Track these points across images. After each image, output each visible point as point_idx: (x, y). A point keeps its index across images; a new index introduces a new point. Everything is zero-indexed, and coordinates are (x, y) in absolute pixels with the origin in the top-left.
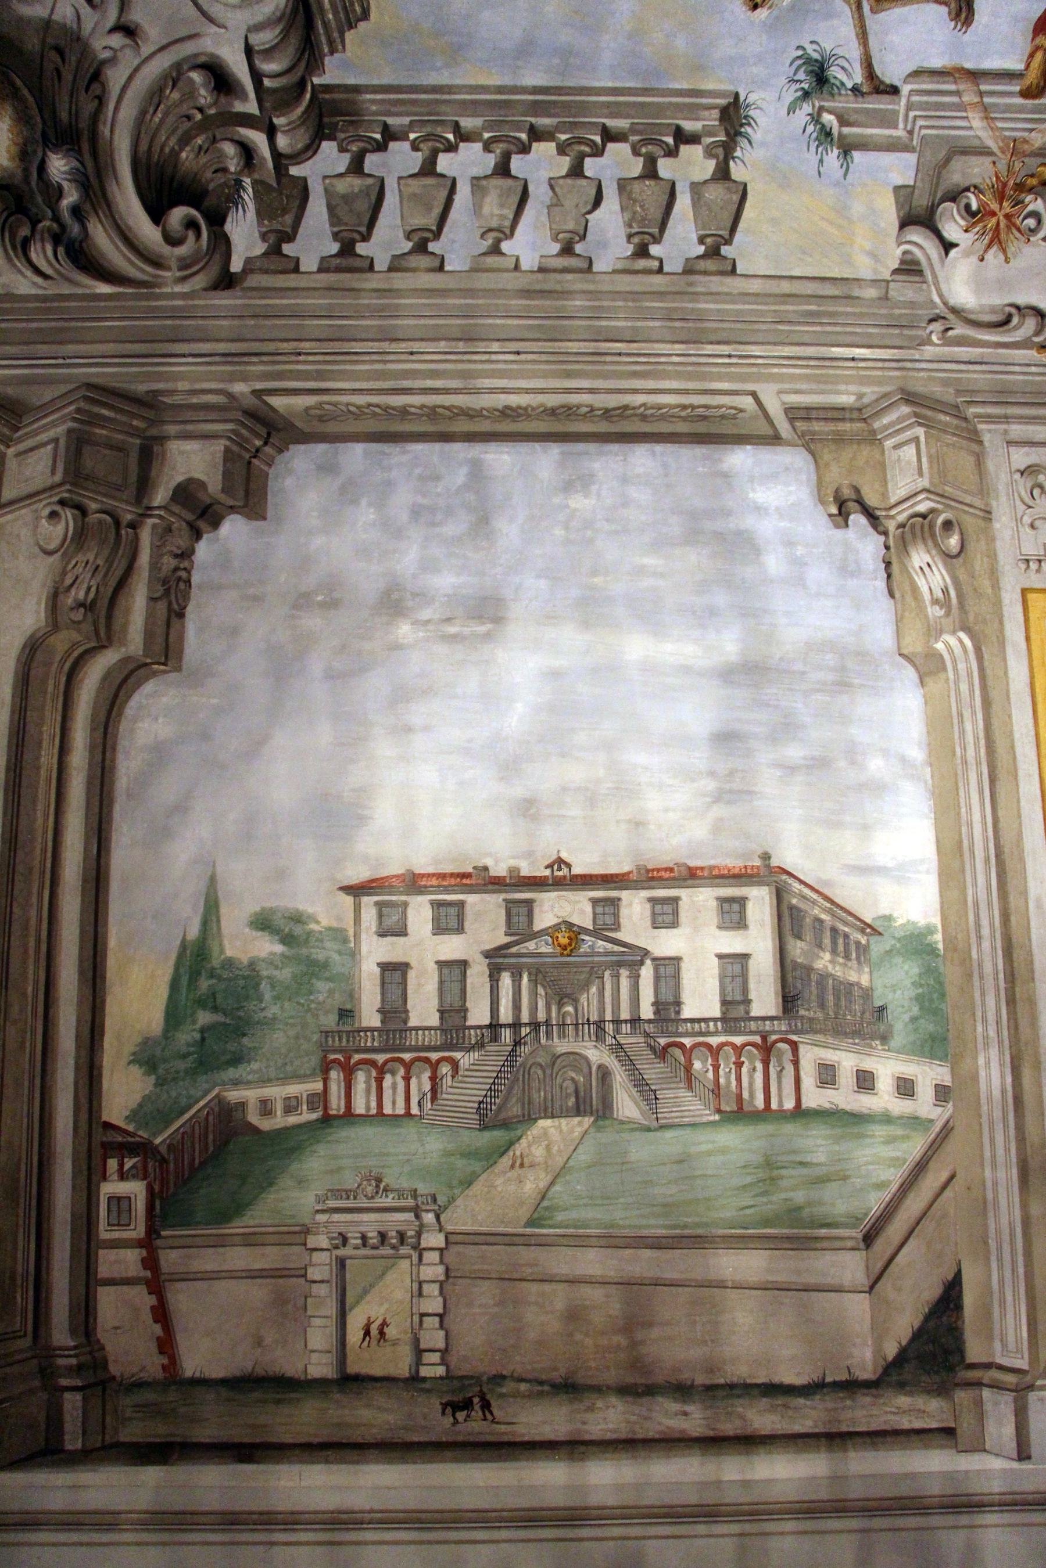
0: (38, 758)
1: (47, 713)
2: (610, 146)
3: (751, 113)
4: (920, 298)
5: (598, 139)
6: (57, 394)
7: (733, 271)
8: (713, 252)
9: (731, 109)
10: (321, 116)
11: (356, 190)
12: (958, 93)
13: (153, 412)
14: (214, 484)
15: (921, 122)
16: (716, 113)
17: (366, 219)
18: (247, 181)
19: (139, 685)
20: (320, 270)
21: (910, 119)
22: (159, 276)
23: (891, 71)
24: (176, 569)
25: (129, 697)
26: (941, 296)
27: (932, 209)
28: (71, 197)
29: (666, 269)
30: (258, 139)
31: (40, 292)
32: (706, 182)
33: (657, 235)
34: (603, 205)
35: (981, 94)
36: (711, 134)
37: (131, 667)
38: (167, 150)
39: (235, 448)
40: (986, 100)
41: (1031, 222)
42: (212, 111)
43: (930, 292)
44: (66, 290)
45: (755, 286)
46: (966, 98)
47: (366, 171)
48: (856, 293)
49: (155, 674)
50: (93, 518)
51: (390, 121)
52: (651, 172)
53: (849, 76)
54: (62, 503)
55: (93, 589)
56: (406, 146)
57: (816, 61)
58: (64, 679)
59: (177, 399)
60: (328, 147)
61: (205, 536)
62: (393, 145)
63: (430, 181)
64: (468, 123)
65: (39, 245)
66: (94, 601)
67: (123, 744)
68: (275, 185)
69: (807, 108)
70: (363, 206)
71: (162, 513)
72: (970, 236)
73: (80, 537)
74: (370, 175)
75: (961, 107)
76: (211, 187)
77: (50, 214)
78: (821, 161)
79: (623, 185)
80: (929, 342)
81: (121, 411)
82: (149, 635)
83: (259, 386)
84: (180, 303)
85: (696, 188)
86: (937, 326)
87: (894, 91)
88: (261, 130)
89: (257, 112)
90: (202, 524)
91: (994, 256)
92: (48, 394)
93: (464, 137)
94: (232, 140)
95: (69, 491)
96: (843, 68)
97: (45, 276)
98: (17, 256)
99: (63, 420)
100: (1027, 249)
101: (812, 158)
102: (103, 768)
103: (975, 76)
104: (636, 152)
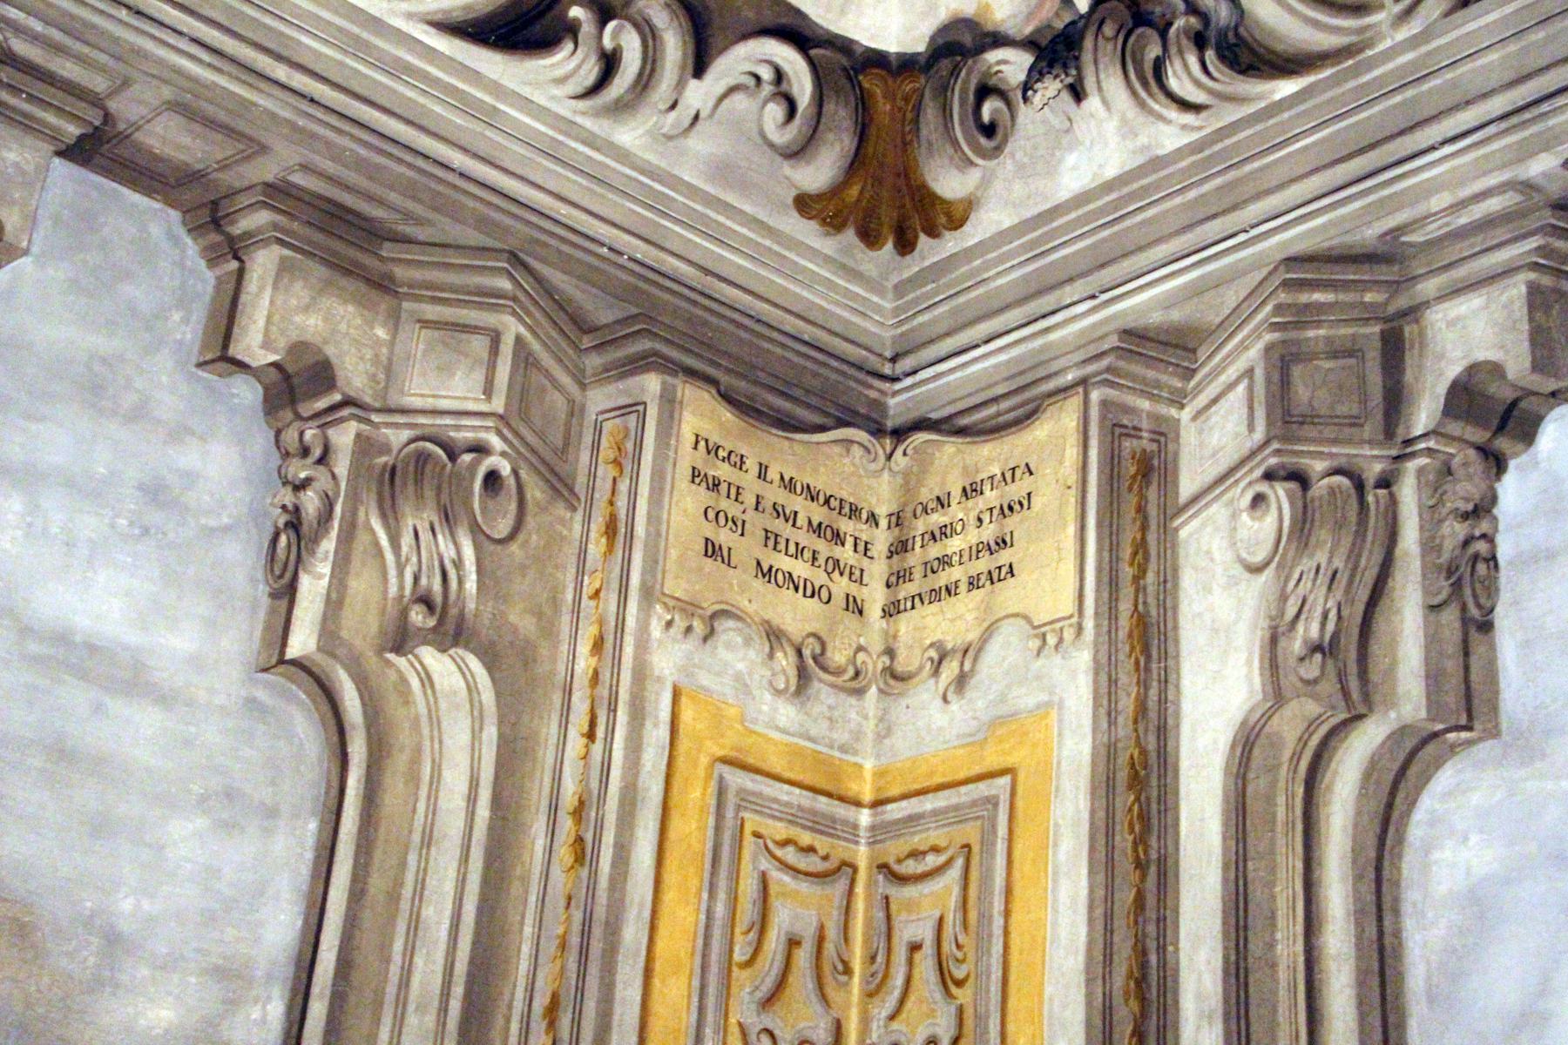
0: (1271, 945)
1: (1280, 859)
13: (1396, 268)
14: (1517, 363)
19: (1425, 779)
22: (1369, 27)
24: (1466, 543)
25: (1412, 803)
31: (1195, 136)
37: (1409, 744)
44: (1233, 114)
49: (1453, 749)
50: (1320, 488)
54: (1269, 476)
55: (1333, 615)
58: (1300, 791)
59: (1433, 230)
61: (1512, 464)
66: (1336, 636)
67: (1411, 897)
71: (1432, 444)
73: (1302, 529)
81: (1345, 285)
82: (1433, 678)
84: (1409, 56)
90: (1502, 444)
92: (1231, 297)
95: (1278, 452)
97: (1195, 108)
98: (1151, 95)
99: (1256, 334)
102: (1381, 950)
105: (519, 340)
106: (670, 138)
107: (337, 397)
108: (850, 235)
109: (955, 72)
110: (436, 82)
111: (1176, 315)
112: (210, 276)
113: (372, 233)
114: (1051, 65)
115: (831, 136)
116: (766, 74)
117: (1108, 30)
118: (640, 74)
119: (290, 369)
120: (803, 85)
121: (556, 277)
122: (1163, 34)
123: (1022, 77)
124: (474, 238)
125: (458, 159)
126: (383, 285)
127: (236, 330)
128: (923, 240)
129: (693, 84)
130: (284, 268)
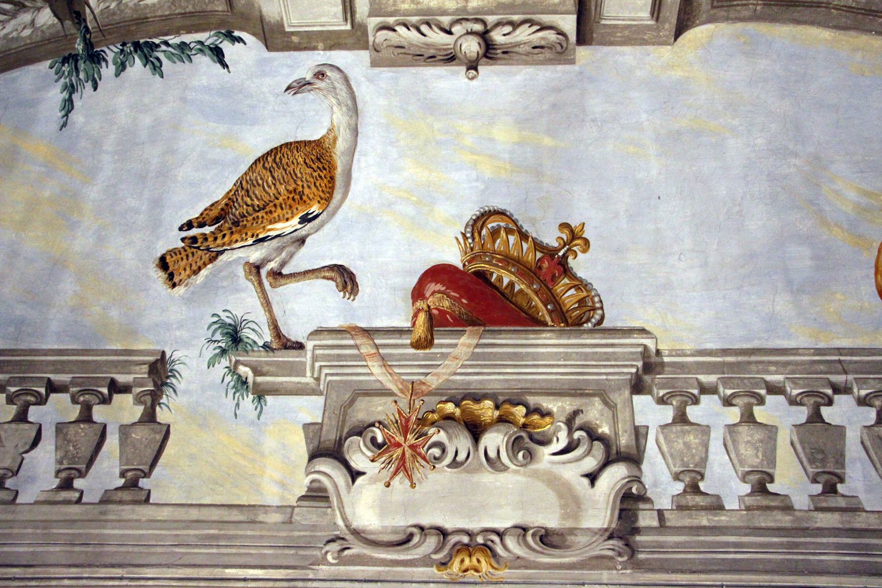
2: (53, 396)
3: (176, 367)
4: (324, 522)
5: (43, 390)
7: (147, 500)
8: (132, 485)
9: (159, 365)
12: (356, 347)
15: (326, 371)
16: (145, 368)
21: (317, 369)
23: (295, 331)
26: (345, 519)
27: (340, 443)
29: (84, 500)
32: (134, 424)
33: (84, 470)
34: (40, 446)
35: (377, 347)
36: (142, 386)
40: (381, 351)
41: (436, 452)
43: (334, 515)
45: (164, 514)
46: (364, 350)
48: (261, 517)
52: (86, 417)
53: (260, 336)
57: (230, 325)
69: (225, 362)
72: (378, 465)
75: (360, 357)
78: (238, 405)
79: (60, 428)
80: (324, 561)
85: (125, 430)
86: (335, 547)
87: (300, 346)
91: (400, 483)
96: (253, 330)
100: (432, 476)
101: (230, 402)
103: (369, 332)
104: (74, 401)
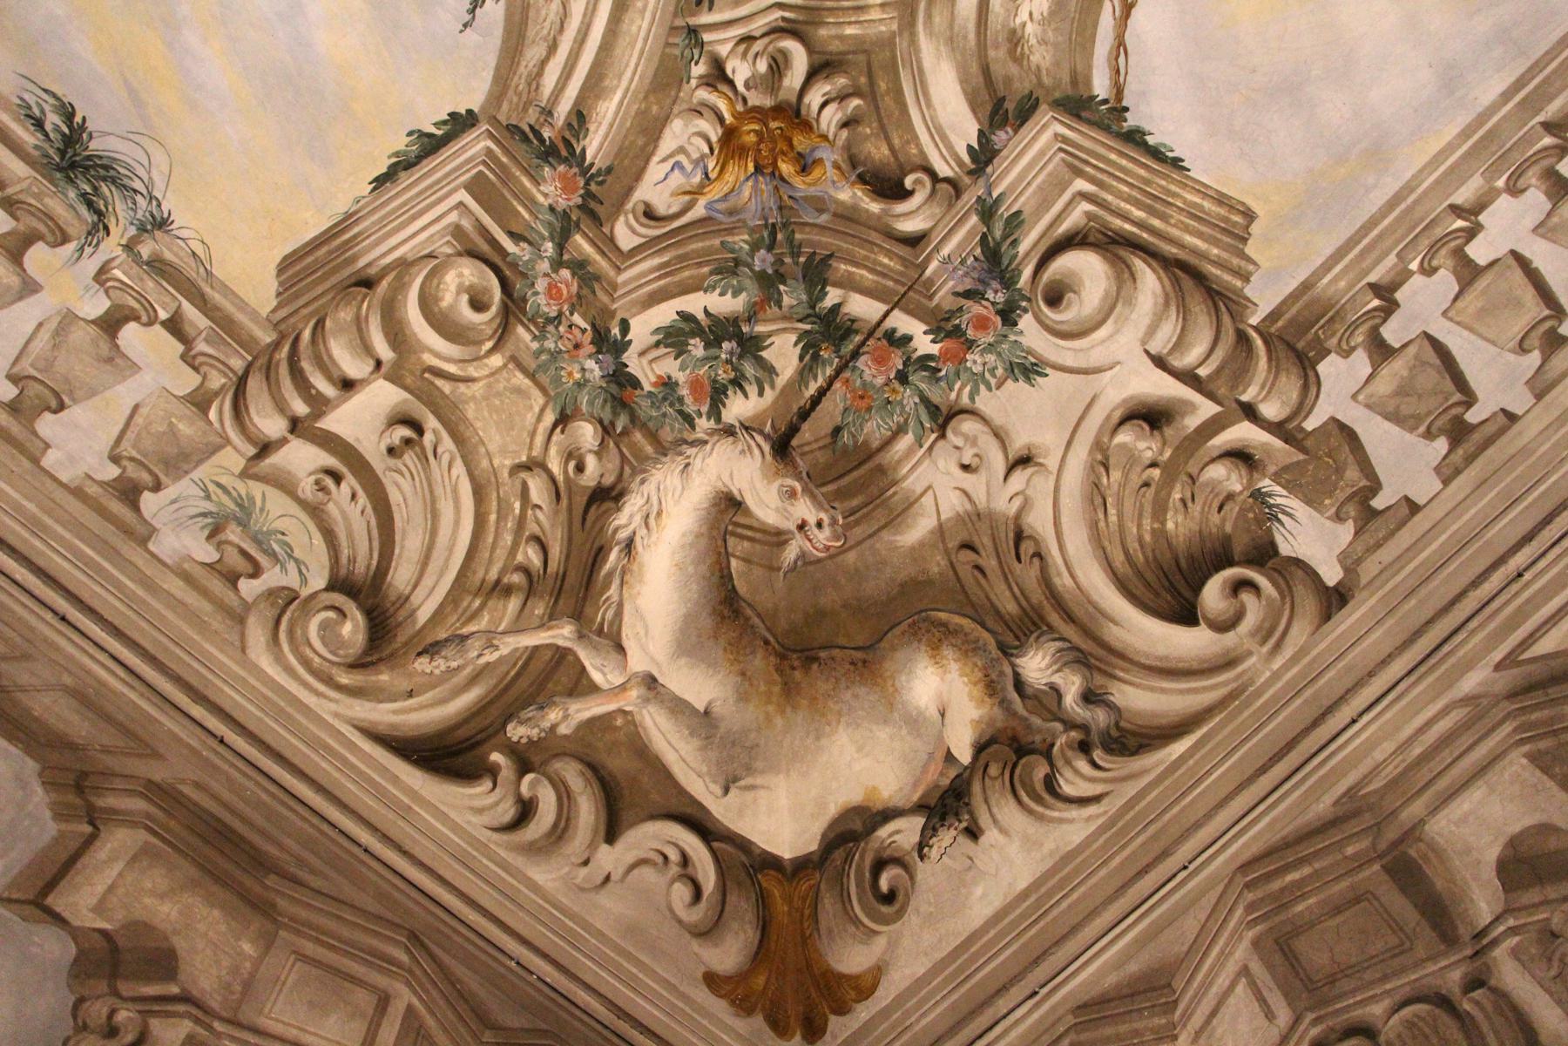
6: (1203, 917)
10: (1291, 347)
11: (1405, 373)
13: (1367, 815)
17: (1448, 385)
18: (1266, 484)
20: (1446, 482)
22: (1244, 672)
28: (1072, 685)
30: (1243, 432)
31: (1100, 821)
38: (1148, 538)
39: (1543, 745)
42: (1168, 453)
44: (1131, 789)
47: (1397, 345)
51: (1373, 278)
56: (1417, 281)
59: (1390, 771)
60: (1328, 368)
62: (1399, 296)
63: (1482, 283)
64: (1463, 195)
65: (1068, 773)
68: (1301, 457)
70: (1432, 378)
71: (1511, 922)
74: (1405, 346)
76: (1228, 528)
77: (1058, 726)
81: (1316, 854)
83: (1498, 655)
84: (1295, 670)
88: (1232, 424)
89: (1218, 409)
93: (1471, 212)
94: (1213, 460)
97: (1096, 799)
98: (1047, 806)
99: (1237, 936)
105: (410, 1009)
106: (582, 889)
107: (175, 990)
108: (758, 1021)
109: (848, 859)
110: (353, 767)
111: (1133, 968)
112: (52, 828)
113: (260, 863)
114: (943, 818)
115: (735, 925)
116: (674, 856)
117: (994, 770)
118: (555, 825)
119: (121, 942)
120: (707, 874)
121: (460, 971)
122: (1047, 754)
123: (916, 838)
124: (372, 905)
125: (365, 837)
126: (262, 908)
127: (63, 883)
128: (834, 1021)
129: (604, 847)
130: (142, 854)
